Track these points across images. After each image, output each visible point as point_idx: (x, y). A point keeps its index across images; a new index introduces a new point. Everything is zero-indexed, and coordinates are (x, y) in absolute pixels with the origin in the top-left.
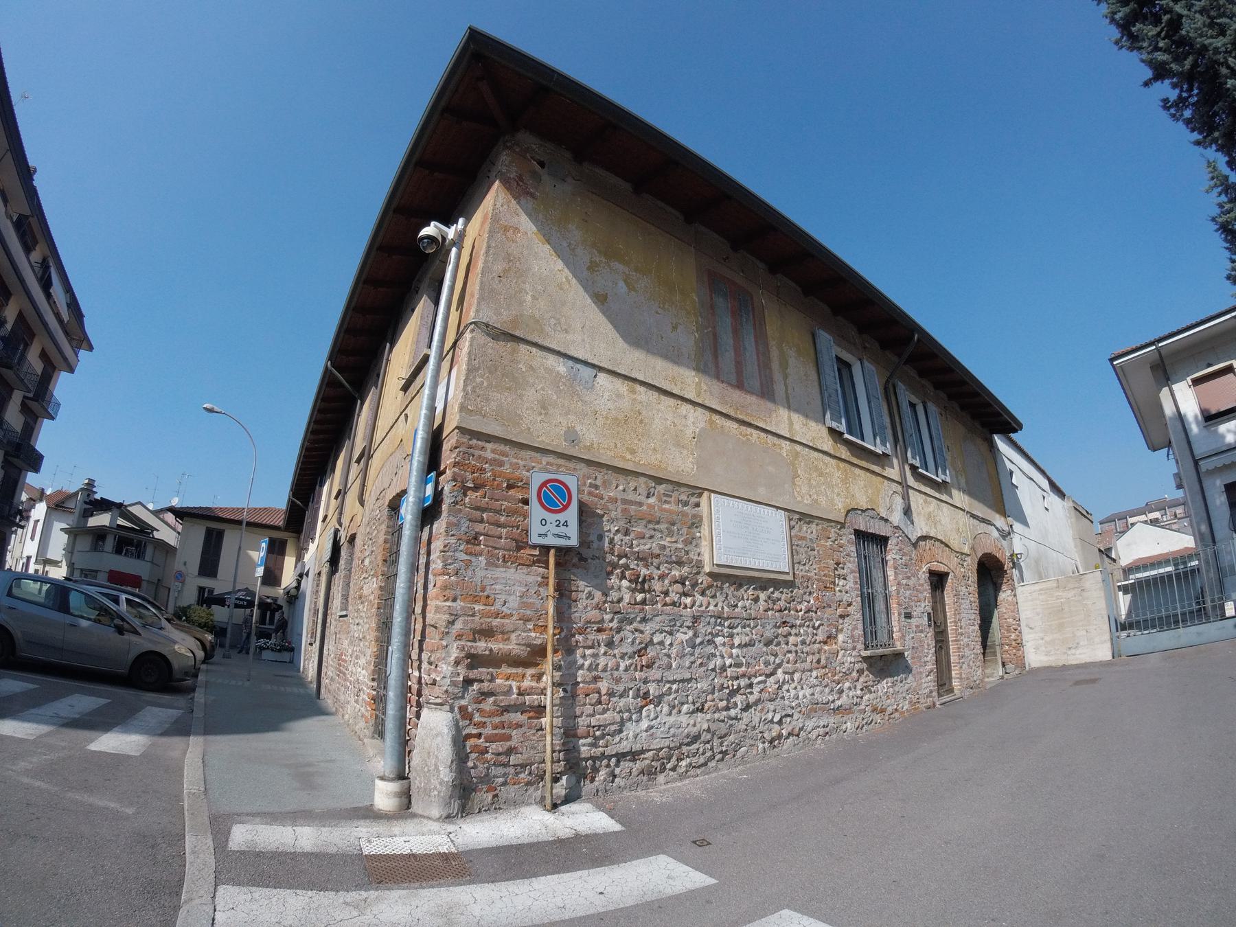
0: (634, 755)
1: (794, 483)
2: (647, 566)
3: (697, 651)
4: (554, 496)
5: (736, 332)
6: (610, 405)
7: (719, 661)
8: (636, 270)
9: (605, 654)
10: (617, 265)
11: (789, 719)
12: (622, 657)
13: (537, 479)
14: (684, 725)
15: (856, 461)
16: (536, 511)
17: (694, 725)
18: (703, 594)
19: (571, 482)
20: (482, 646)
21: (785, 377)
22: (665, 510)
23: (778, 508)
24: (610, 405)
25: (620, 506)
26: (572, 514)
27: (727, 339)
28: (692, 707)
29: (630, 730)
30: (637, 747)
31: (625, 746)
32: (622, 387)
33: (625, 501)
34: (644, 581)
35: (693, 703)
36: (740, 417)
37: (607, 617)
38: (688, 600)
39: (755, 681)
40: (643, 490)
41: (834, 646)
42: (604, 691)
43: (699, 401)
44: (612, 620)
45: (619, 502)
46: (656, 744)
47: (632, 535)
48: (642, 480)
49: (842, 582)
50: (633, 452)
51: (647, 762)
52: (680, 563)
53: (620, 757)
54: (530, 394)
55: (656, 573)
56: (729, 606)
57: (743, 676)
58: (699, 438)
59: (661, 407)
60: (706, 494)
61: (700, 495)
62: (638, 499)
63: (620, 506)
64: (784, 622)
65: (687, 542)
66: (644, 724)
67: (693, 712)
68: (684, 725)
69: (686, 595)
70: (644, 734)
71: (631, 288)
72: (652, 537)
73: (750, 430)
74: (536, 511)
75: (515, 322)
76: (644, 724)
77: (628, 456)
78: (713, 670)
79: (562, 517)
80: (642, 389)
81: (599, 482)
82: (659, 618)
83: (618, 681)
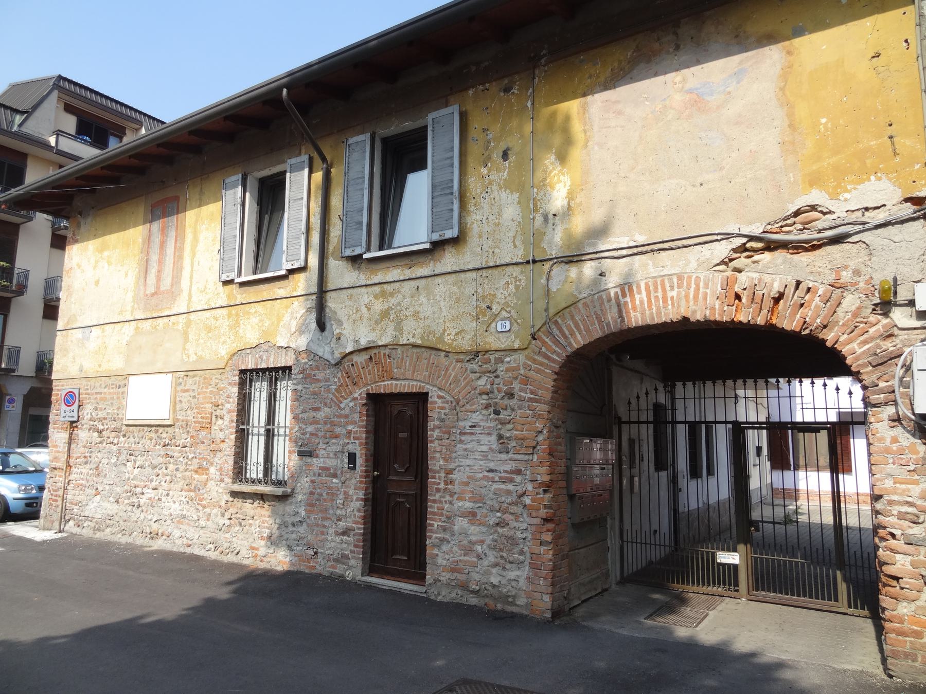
18: (124, 436)
21: (194, 254)
39: (145, 490)
49: (220, 422)
65: (118, 408)
71: (109, 263)
79: (72, 408)
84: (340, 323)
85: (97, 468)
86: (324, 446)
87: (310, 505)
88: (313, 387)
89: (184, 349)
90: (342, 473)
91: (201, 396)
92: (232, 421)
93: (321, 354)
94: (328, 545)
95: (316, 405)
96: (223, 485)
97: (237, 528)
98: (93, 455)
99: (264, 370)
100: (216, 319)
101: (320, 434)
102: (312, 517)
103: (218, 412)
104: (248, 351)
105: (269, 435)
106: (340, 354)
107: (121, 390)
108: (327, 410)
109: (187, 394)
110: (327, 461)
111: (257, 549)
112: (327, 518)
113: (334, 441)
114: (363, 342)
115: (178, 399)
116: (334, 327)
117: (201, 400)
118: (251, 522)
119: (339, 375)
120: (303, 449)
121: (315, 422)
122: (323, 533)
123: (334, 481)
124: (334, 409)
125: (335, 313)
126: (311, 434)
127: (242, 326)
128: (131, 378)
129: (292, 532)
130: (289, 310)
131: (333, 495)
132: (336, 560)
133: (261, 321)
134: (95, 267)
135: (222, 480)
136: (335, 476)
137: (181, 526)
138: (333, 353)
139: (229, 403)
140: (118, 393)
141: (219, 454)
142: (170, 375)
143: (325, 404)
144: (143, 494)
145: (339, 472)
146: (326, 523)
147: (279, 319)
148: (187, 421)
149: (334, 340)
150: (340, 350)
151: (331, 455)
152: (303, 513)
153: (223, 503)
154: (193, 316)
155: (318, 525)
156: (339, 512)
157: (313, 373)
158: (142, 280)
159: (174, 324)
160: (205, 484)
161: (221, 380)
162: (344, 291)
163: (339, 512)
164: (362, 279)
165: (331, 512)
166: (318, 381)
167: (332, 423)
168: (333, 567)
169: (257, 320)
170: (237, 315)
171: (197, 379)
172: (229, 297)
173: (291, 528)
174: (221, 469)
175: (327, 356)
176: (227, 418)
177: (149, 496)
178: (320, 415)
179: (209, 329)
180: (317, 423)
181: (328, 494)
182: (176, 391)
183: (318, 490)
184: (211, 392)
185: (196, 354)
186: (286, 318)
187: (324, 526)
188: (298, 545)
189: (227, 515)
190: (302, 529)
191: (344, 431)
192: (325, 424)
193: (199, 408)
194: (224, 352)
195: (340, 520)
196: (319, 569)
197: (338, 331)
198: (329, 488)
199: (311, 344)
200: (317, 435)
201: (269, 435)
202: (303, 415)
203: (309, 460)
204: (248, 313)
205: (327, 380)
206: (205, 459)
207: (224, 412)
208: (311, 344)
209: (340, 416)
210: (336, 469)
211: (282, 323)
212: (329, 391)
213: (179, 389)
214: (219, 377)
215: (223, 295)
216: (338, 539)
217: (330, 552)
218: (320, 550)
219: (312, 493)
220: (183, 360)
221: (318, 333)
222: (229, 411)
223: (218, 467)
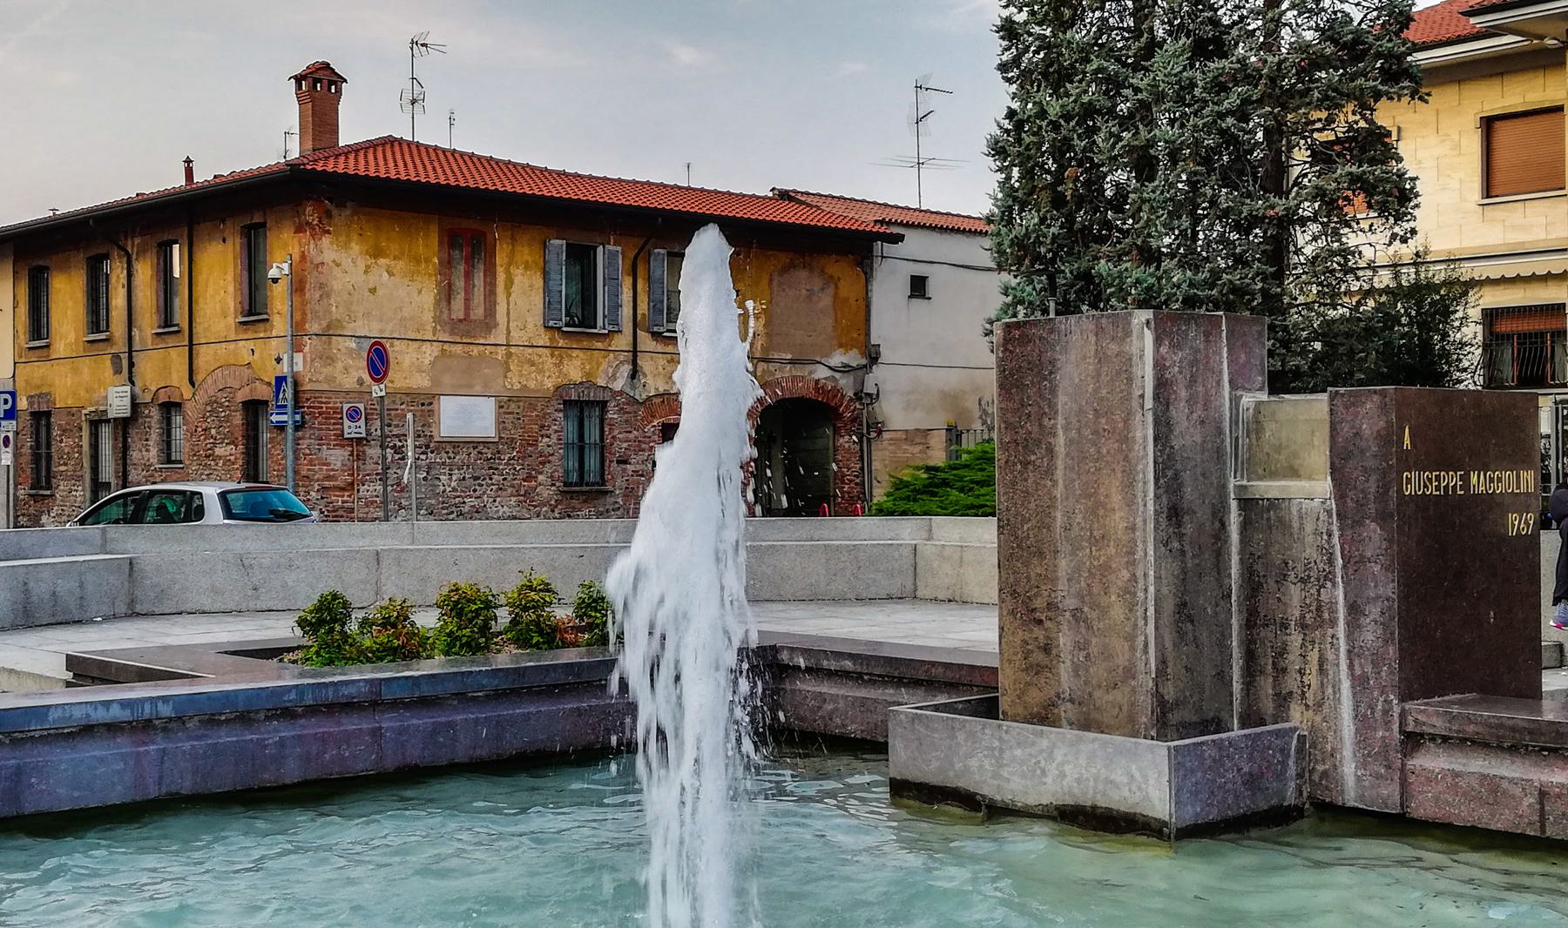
4: (354, 415)
5: (468, 276)
8: (395, 258)
10: (382, 261)
13: (346, 407)
16: (347, 423)
19: (361, 406)
20: (327, 484)
21: (509, 295)
26: (362, 422)
27: (460, 283)
49: (546, 440)
54: (340, 365)
58: (432, 363)
71: (391, 274)
74: (347, 423)
75: (329, 327)
84: (645, 375)
85: (398, 484)
87: (626, 496)
114: (661, 390)
134: (366, 272)
147: (599, 365)
154: (513, 350)
158: (444, 304)
164: (660, 348)
176: (554, 437)
178: (631, 436)
186: (604, 365)
194: (549, 384)
215: (544, 339)
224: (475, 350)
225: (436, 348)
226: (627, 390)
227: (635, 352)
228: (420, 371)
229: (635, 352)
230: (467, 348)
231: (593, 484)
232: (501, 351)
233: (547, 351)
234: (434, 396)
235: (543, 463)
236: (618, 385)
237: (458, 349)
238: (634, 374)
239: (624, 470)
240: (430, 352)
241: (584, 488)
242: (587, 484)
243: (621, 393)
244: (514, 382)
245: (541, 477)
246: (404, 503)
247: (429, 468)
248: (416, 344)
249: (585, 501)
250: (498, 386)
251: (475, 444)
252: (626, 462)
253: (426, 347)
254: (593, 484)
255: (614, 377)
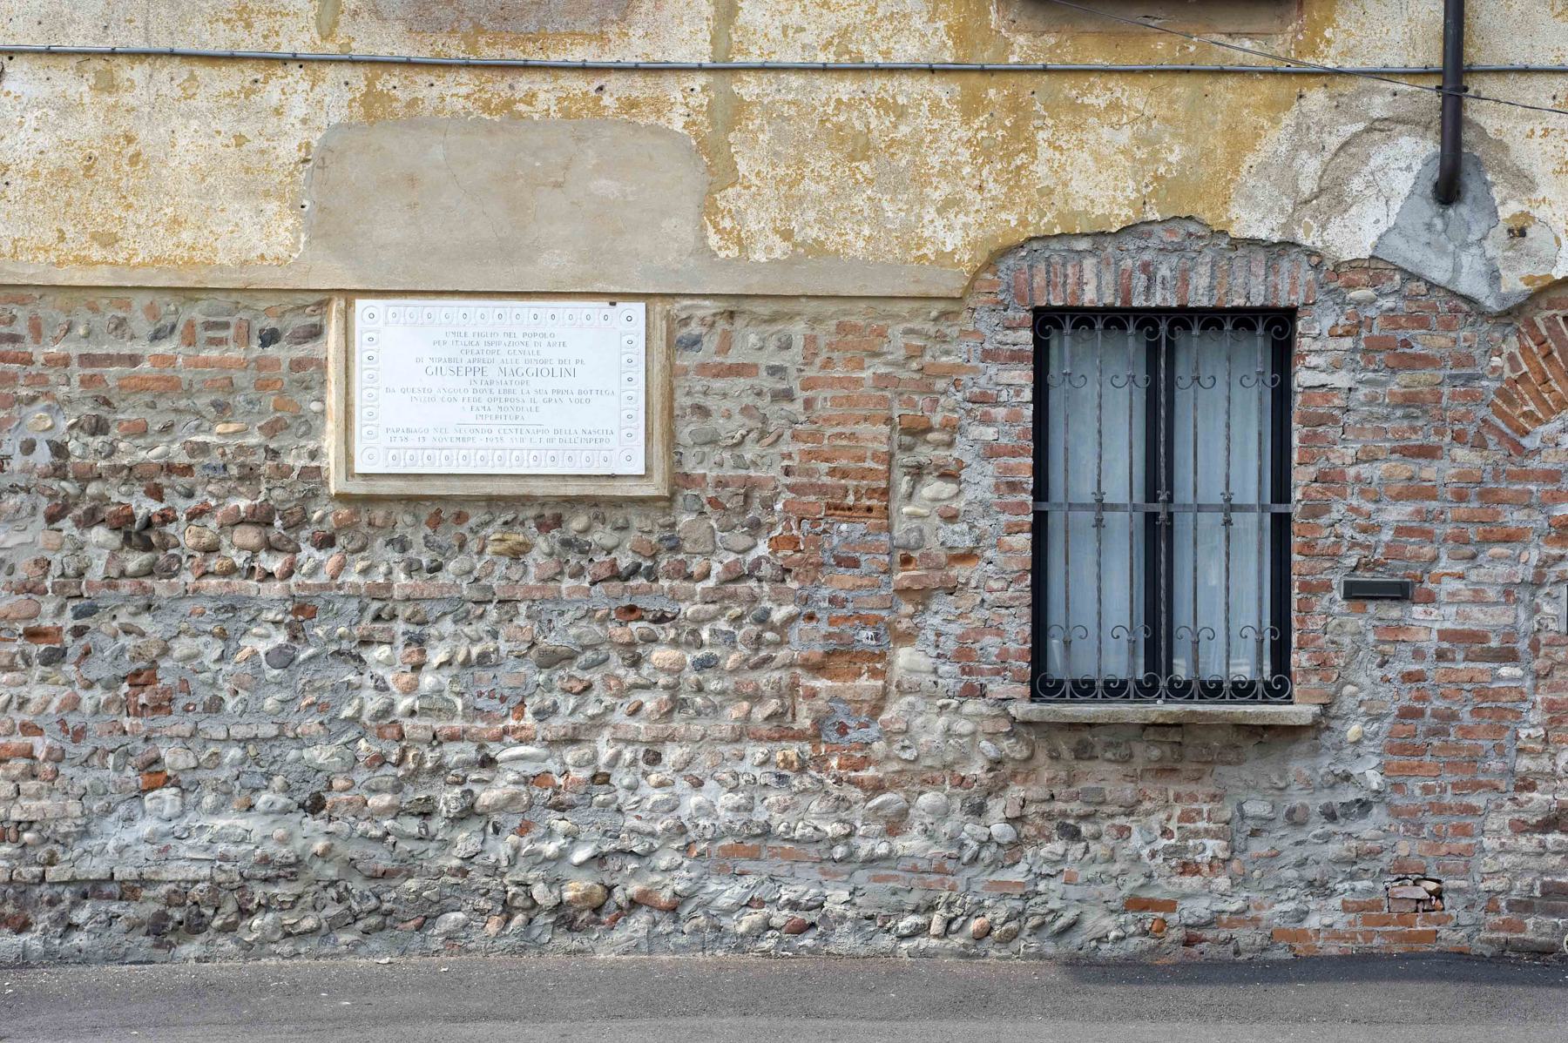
0: (130, 891)
1: (709, 209)
2: (156, 493)
3: (302, 679)
6: (43, 140)
7: (374, 702)
9: (43, 679)
11: (633, 865)
12: (89, 686)
14: (256, 837)
15: (1068, 56)
17: (283, 841)
18: (326, 542)
22: (207, 363)
23: (614, 298)
24: (43, 140)
25: (77, 372)
28: (282, 800)
29: (113, 834)
30: (125, 872)
31: (94, 868)
32: (69, 83)
33: (87, 360)
34: (148, 524)
35: (287, 788)
36: (489, 54)
37: (49, 606)
38: (275, 564)
40: (141, 324)
41: (865, 682)
42: (40, 753)
43: (331, 49)
44: (60, 610)
45: (75, 365)
46: (175, 871)
47: (115, 432)
48: (140, 301)
49: (933, 488)
50: (108, 240)
51: (155, 908)
52: (249, 475)
53: (89, 890)
55: (183, 506)
56: (412, 568)
57: (454, 738)
59: (200, 102)
60: (337, 305)
61: (323, 305)
62: (127, 349)
63: (77, 372)
64: (632, 609)
65: (272, 429)
66: (145, 827)
67: (286, 811)
68: (256, 837)
69: (271, 547)
70: (145, 849)
72: (167, 429)
73: (524, 83)
76: (145, 827)
77: (96, 253)
78: (353, 720)
80: (137, 72)
81: (21, 328)
82: (187, 606)
83: (78, 735)
84: (1523, 181)
86: (1459, 568)
87: (1403, 751)
88: (1399, 383)
89: (709, 209)
90: (1535, 647)
91: (821, 394)
92: (1013, 487)
93: (1439, 275)
94: (1487, 863)
95: (1416, 439)
96: (971, 706)
97: (1058, 846)
98: (104, 625)
99: (1148, 318)
100: (901, 113)
101: (1439, 530)
102: (1415, 786)
103: (924, 454)
104: (1083, 245)
105: (1157, 538)
106: (1530, 280)
107: (281, 352)
108: (1461, 453)
109: (743, 383)
110: (1475, 611)
111: (1170, 906)
112: (1477, 786)
113: (1497, 550)
115: (682, 401)
116: (1497, 193)
117: (822, 408)
118: (1121, 821)
119: (1512, 346)
120: (1365, 576)
121: (1415, 491)
122: (1464, 831)
123: (1505, 671)
124: (1496, 452)
125: (1505, 148)
126: (1400, 531)
127: (1044, 152)
128: (360, 304)
129: (1326, 838)
130: (1288, 119)
131: (1498, 713)
132: (1524, 906)
133: (1141, 140)
135: (974, 692)
136: (1508, 655)
137: (746, 865)
138: (1494, 277)
139: (987, 421)
140: (260, 364)
141: (942, 605)
142: (639, 308)
143: (1458, 438)
144: (488, 762)
145: (1523, 645)
146: (1477, 800)
148: (748, 490)
149: (1500, 233)
150: (1526, 270)
151: (1492, 594)
152: (1375, 780)
153: (976, 769)
154: (749, 88)
155: (1439, 809)
156: (1524, 764)
157: (1401, 335)
159: (633, 104)
160: (877, 709)
161: (942, 338)
162: (1539, 81)
163: (1524, 764)
165: (1495, 764)
166: (1427, 361)
167: (1485, 495)
168: (1508, 926)
169: (1124, 137)
170: (1014, 106)
171: (798, 329)
172: (960, 35)
173: (1318, 827)
174: (963, 655)
175: (1471, 283)
176: (981, 481)
177: (530, 769)
179: (860, 148)
180: (1430, 494)
181: (1477, 711)
182: (672, 373)
183: (1439, 704)
184: (882, 381)
185: (787, 235)
186: (1275, 140)
187: (1471, 810)
188: (1352, 877)
189: (997, 809)
190: (1367, 828)
191: (1539, 520)
192: (1461, 497)
193: (815, 436)
194: (953, 237)
195: (1531, 787)
196: (1451, 937)
197: (1509, 210)
198: (1482, 693)
199: (1396, 241)
200: (1428, 536)
201: (1157, 538)
202: (1365, 470)
203: (1394, 612)
204: (1075, 107)
205: (1466, 360)
206: (866, 622)
207: (962, 450)
208: (1396, 241)
209: (1525, 476)
210: (1510, 634)
211: (1250, 159)
212: (1474, 397)
213: (688, 359)
214: (931, 328)
216: (1527, 843)
217: (1495, 884)
218: (1449, 883)
219: (1407, 713)
220: (703, 249)
221: (1427, 210)
222: (991, 452)
223: (950, 646)
224: (545, 93)
225: (336, 95)
226: (1411, 254)
227: (1455, 76)
228: (251, 189)
229: (1455, 76)
230: (500, 86)
231: (1212, 691)
232: (683, 102)
233: (939, 89)
234: (322, 299)
235: (920, 596)
236: (1354, 235)
237: (456, 90)
238: (1448, 188)
239: (1394, 632)
240: (305, 108)
241: (1161, 709)
242: (1181, 691)
243: (1375, 268)
244: (760, 233)
245: (904, 657)
246: (173, 757)
247: (302, 611)
248: (232, 78)
249: (1165, 771)
250: (668, 248)
251: (550, 510)
252: (1401, 593)
253: (290, 92)
254: (1212, 691)
255: (1332, 196)
